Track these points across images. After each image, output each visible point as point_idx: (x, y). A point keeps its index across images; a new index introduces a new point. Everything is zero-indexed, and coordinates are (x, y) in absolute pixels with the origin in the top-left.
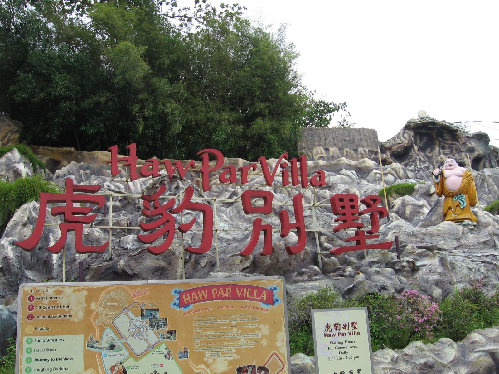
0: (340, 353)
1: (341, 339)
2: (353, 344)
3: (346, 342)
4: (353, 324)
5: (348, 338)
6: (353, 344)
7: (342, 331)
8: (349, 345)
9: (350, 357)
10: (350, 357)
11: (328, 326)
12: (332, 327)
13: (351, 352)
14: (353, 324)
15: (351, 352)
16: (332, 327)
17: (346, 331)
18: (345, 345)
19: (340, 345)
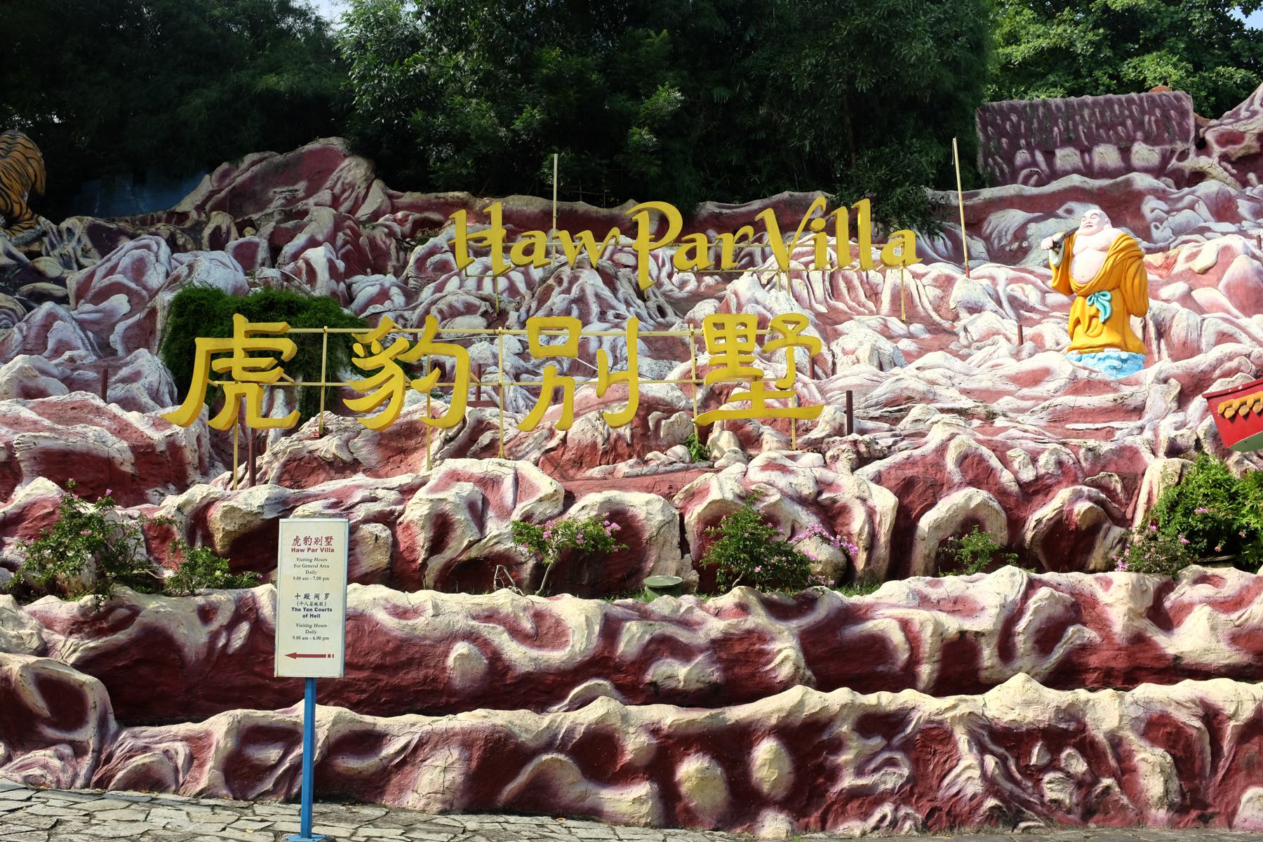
0: (307, 572)
1: (310, 555)
2: (323, 563)
3: (316, 559)
4: (327, 538)
5: (318, 554)
6: (323, 563)
7: (313, 546)
8: (320, 563)
9: (319, 578)
10: (319, 578)
11: (297, 540)
12: (301, 541)
13: (322, 573)
14: (327, 538)
15: (322, 573)
16: (301, 541)
17: (318, 547)
18: (314, 563)
19: (307, 563)
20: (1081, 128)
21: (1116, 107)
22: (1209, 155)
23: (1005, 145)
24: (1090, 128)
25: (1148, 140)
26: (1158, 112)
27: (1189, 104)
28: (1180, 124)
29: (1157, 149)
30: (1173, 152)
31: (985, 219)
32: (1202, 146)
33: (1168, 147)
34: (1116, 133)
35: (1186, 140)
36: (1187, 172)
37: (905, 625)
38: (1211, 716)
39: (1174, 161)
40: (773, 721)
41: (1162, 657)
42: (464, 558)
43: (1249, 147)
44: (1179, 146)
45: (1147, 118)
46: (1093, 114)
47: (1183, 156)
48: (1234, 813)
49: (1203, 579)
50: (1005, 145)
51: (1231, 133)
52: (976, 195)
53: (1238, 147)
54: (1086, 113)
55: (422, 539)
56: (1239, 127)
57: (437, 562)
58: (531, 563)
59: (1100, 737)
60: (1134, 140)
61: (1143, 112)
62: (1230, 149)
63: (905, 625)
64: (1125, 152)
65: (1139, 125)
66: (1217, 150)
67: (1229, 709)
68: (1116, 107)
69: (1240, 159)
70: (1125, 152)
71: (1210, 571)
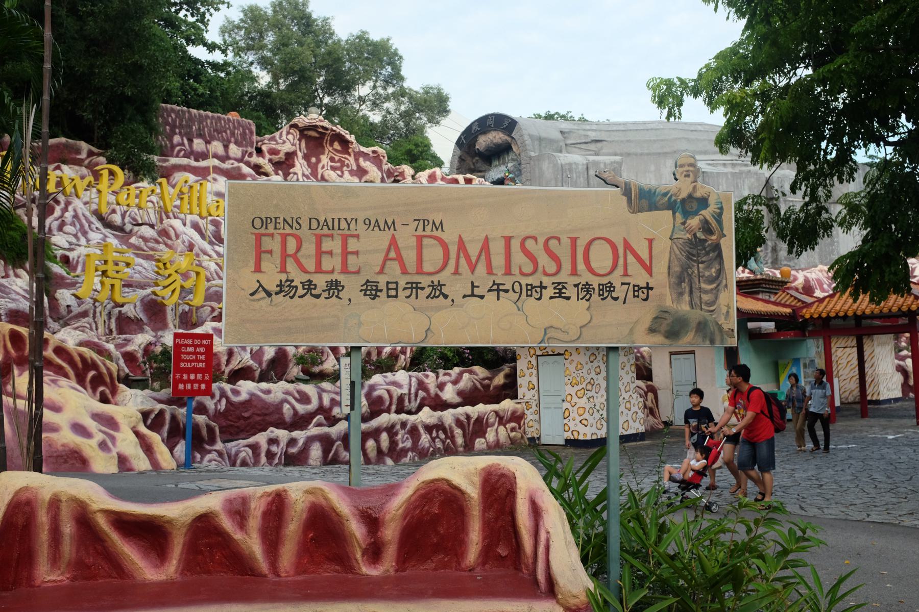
20: (206, 129)
21: (223, 122)
22: (263, 157)
23: (168, 131)
24: (210, 131)
25: (236, 143)
26: (241, 129)
27: (254, 128)
28: (250, 138)
29: (240, 149)
30: (246, 152)
31: (171, 175)
32: (259, 151)
33: (245, 149)
34: (222, 136)
35: (252, 147)
36: (252, 164)
37: (388, 391)
38: (468, 417)
39: (246, 157)
40: (385, 426)
41: (442, 400)
42: (236, 368)
43: (281, 158)
44: (250, 150)
45: (236, 131)
46: (212, 123)
47: (251, 155)
48: (474, 447)
49: (445, 374)
50: (168, 131)
51: (274, 149)
52: (168, 161)
53: (277, 157)
54: (209, 121)
55: (224, 359)
56: (278, 147)
57: (227, 371)
58: (259, 370)
59: (447, 426)
60: (230, 142)
61: (234, 127)
62: (273, 157)
63: (388, 391)
64: (226, 147)
65: (233, 134)
66: (268, 156)
67: (472, 415)
68: (223, 122)
69: (276, 163)
70: (226, 147)
71: (447, 371)
